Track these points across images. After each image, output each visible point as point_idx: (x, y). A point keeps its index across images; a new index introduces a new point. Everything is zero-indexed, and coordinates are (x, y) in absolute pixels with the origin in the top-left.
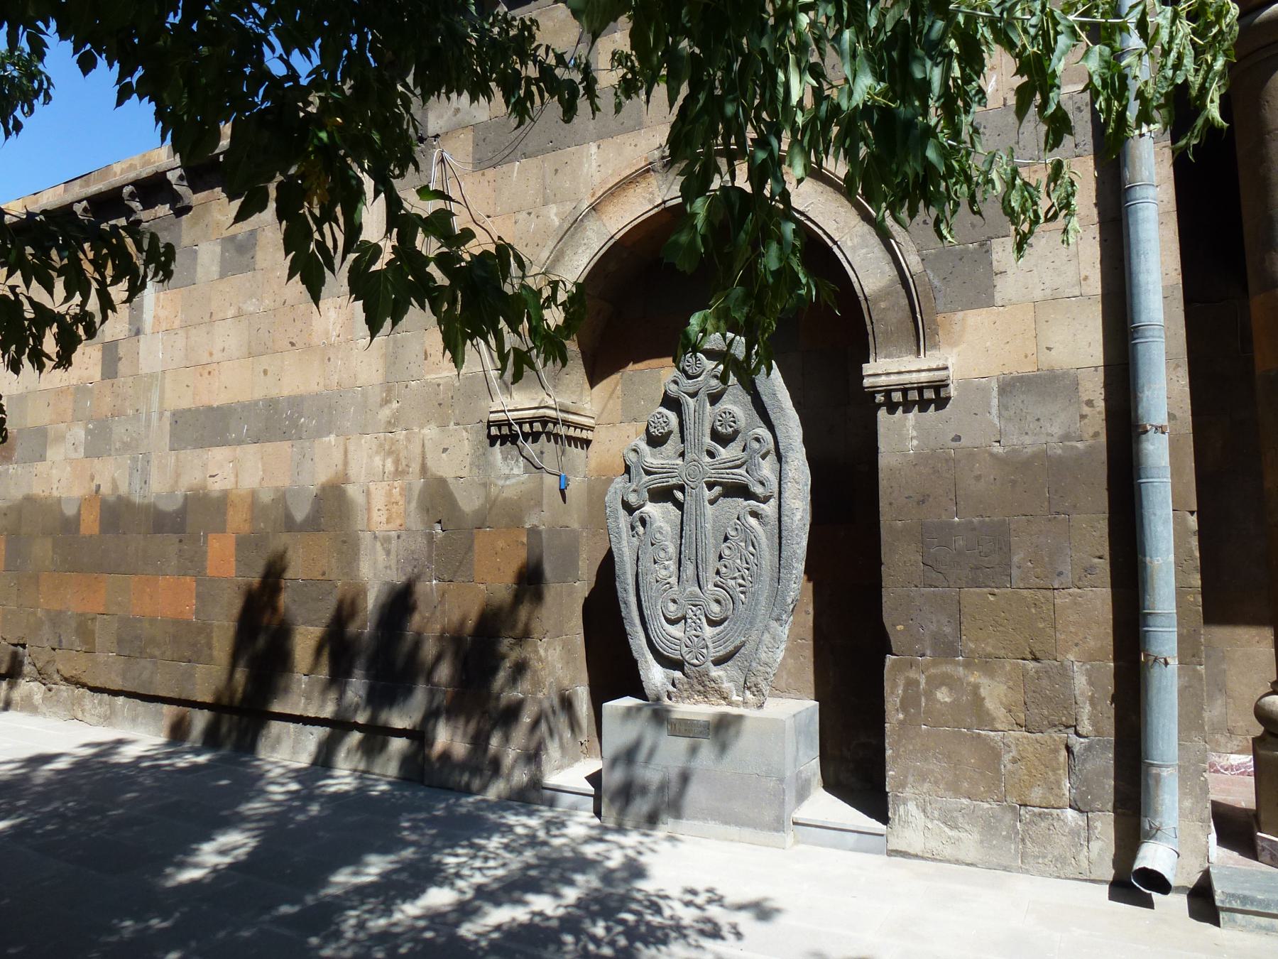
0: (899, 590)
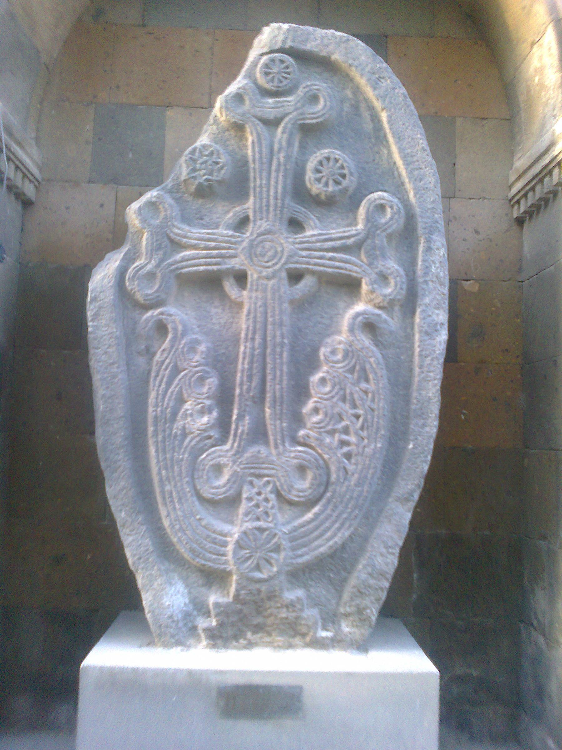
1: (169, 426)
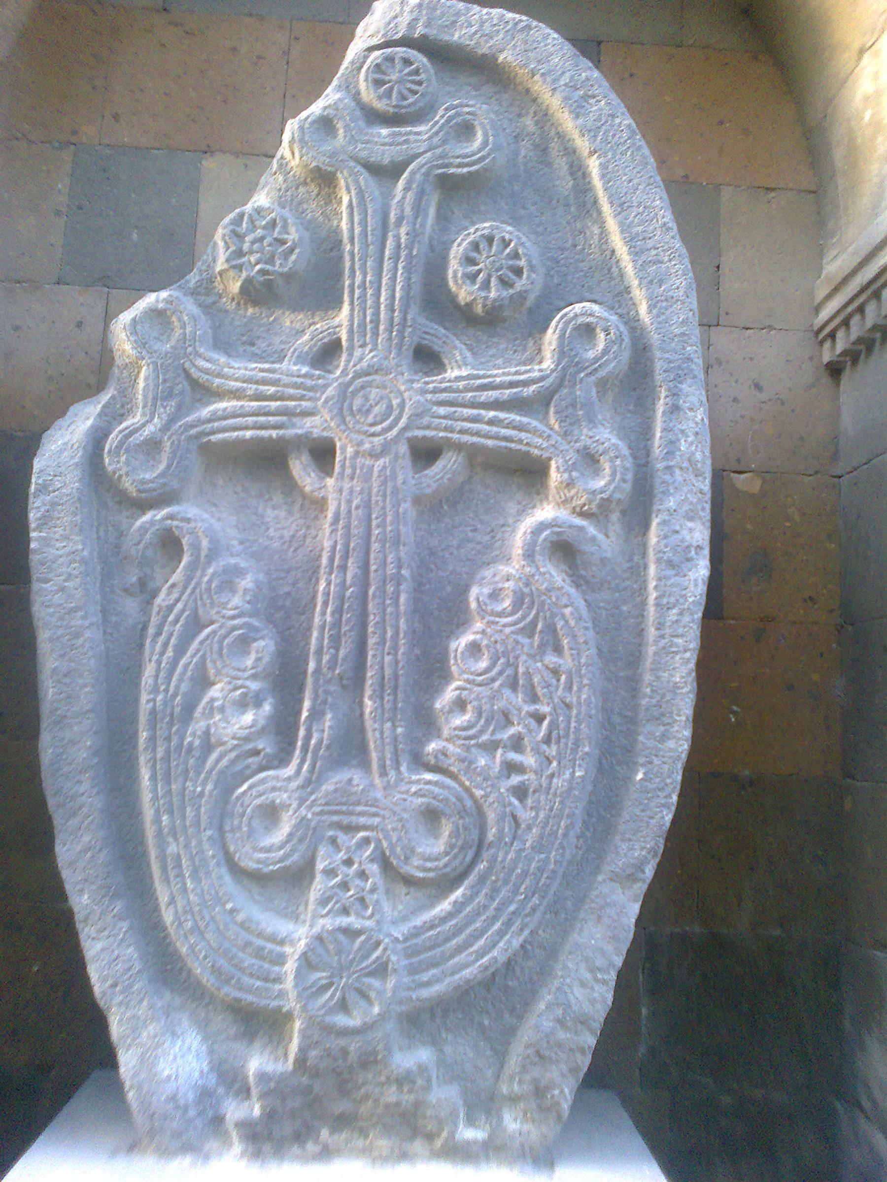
1: (178, 730)
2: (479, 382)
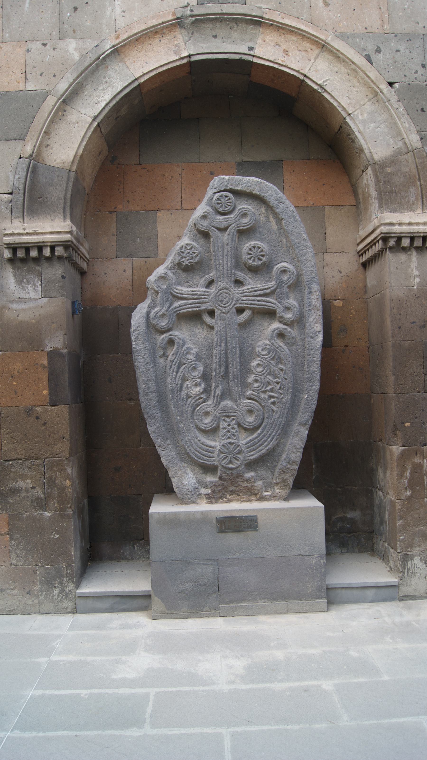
0: (407, 395)
2: (254, 289)
